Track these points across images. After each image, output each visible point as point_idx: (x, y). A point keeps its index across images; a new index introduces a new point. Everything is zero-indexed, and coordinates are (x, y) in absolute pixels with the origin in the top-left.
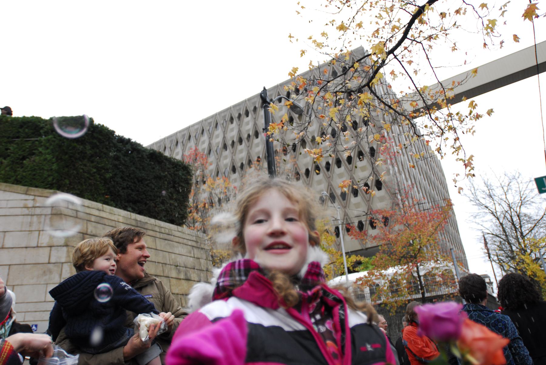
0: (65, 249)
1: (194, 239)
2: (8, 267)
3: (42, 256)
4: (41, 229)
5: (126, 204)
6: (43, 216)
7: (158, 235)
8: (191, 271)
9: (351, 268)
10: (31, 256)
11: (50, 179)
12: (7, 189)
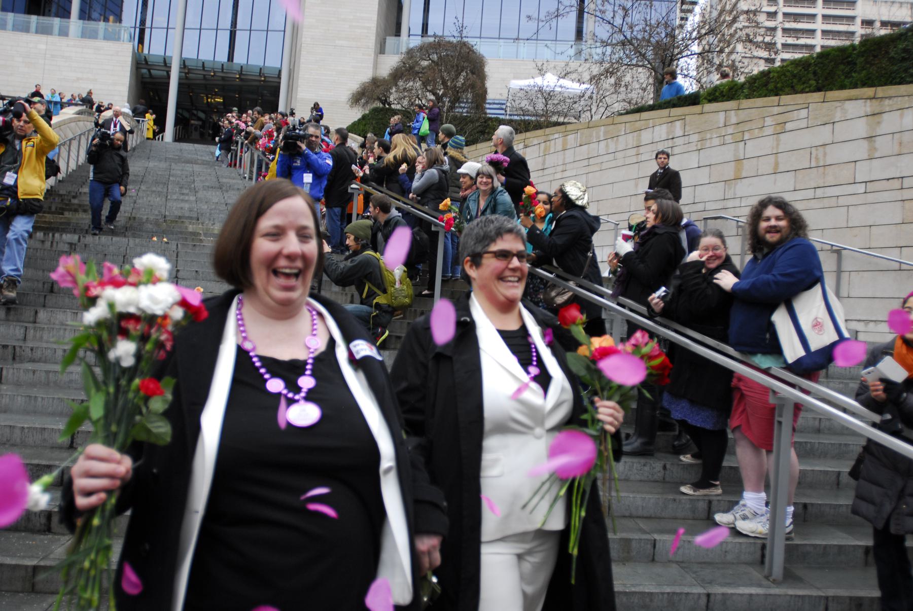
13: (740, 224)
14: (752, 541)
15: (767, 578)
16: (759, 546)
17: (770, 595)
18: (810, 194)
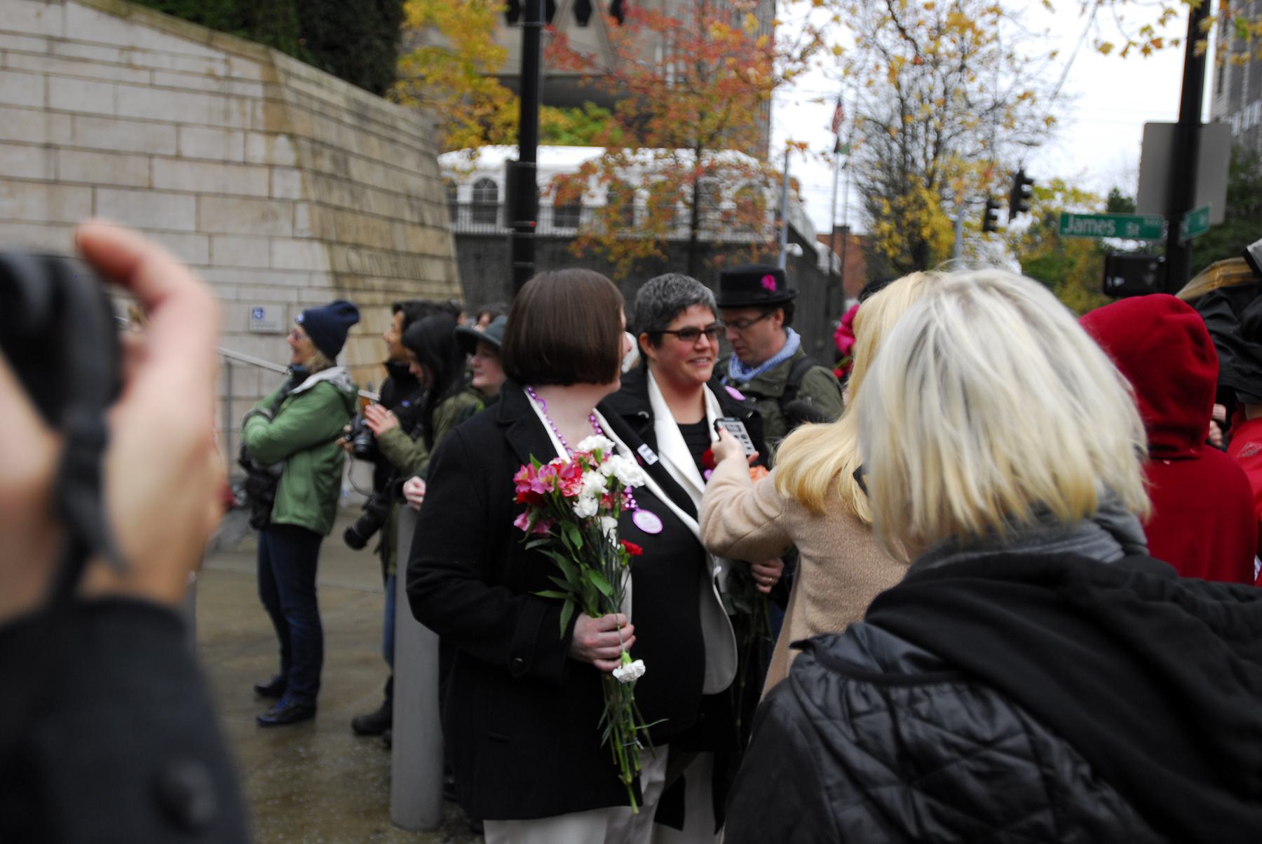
0: (297, 175)
1: (419, 134)
3: (257, 183)
4: (248, 127)
7: (383, 132)
8: (425, 206)
10: (236, 181)
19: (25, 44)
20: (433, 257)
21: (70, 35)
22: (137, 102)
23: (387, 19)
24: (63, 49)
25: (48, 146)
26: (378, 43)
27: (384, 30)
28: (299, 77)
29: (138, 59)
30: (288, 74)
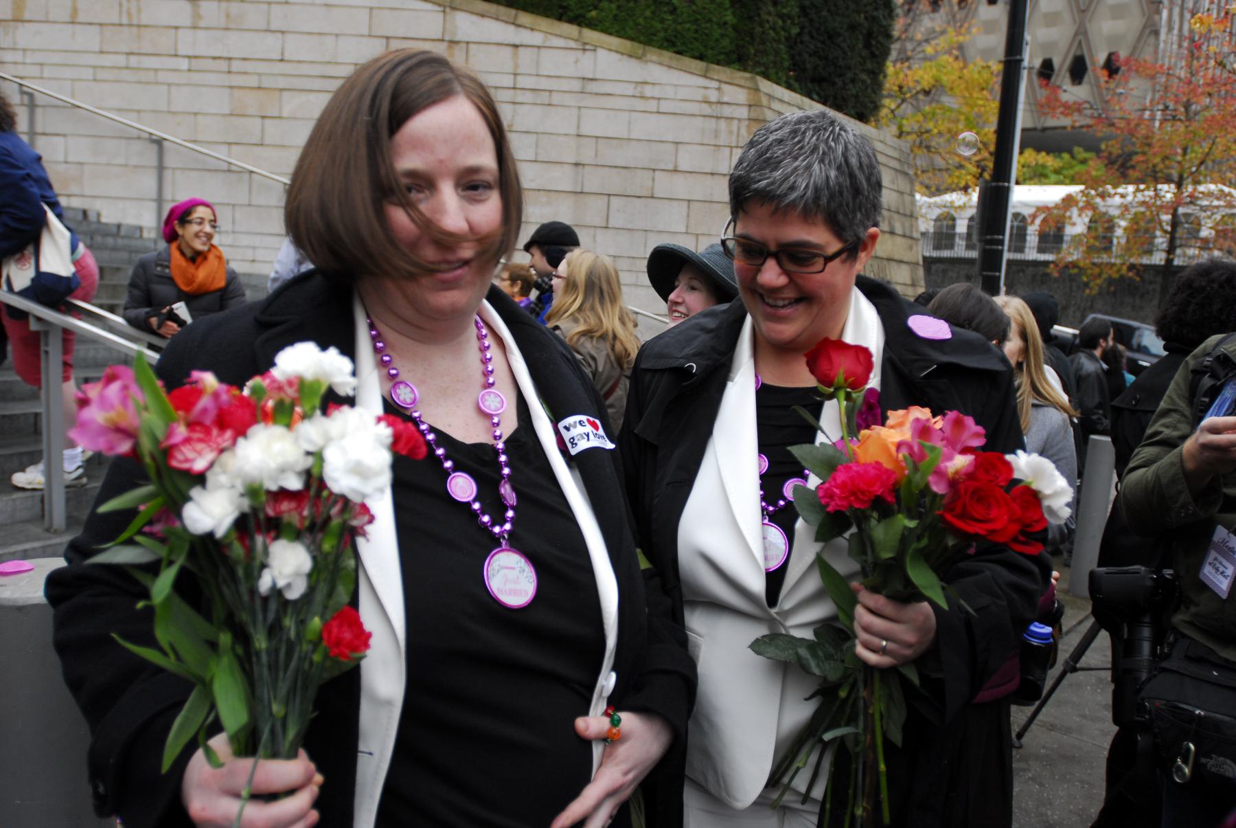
1: (896, 155)
2: (685, 204)
5: (810, 85)
6: (736, 122)
8: (896, 216)
9: (1021, 179)
11: (725, 42)
12: (674, 63)
13: (25, 89)
14: (28, 494)
15: (48, 530)
16: (39, 499)
17: (50, 546)
18: (121, 60)
19: (565, 85)
20: (901, 262)
21: (598, 77)
22: (648, 126)
23: (873, 55)
24: (593, 87)
25: (577, 164)
26: (864, 77)
27: (869, 65)
28: (782, 101)
29: (648, 91)
30: (771, 97)
